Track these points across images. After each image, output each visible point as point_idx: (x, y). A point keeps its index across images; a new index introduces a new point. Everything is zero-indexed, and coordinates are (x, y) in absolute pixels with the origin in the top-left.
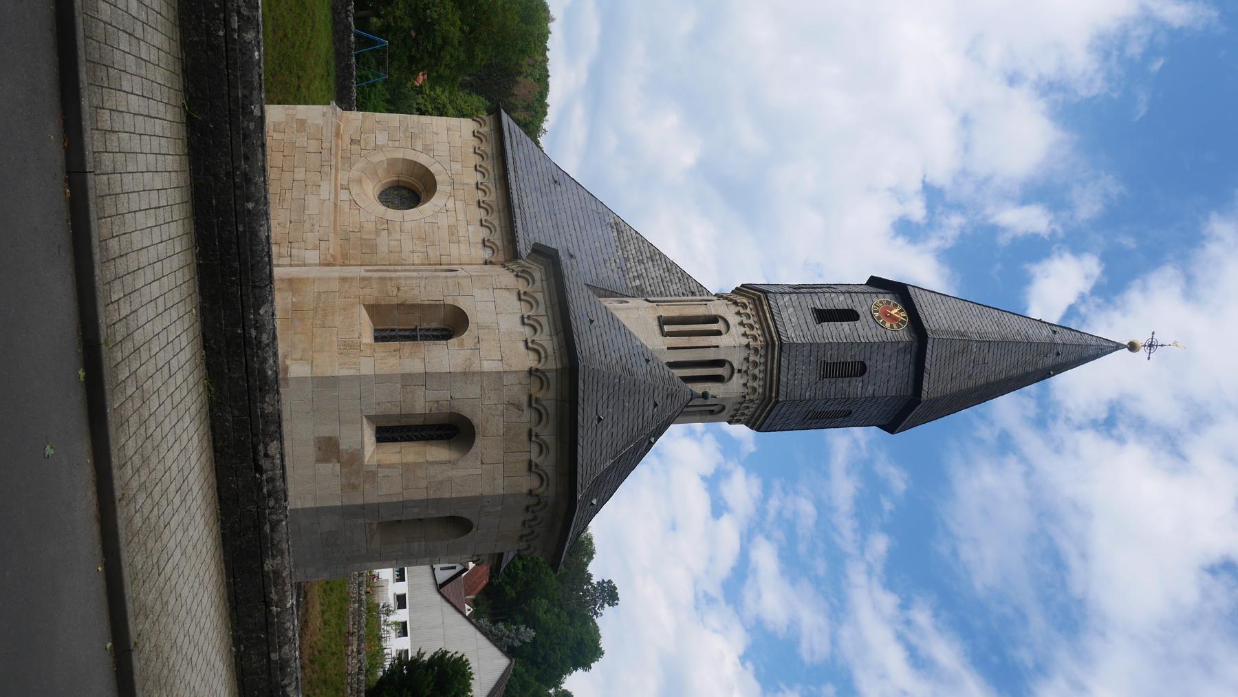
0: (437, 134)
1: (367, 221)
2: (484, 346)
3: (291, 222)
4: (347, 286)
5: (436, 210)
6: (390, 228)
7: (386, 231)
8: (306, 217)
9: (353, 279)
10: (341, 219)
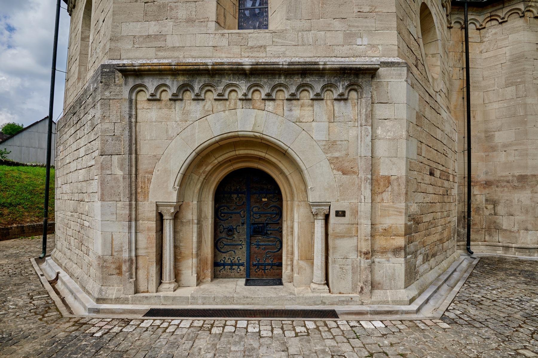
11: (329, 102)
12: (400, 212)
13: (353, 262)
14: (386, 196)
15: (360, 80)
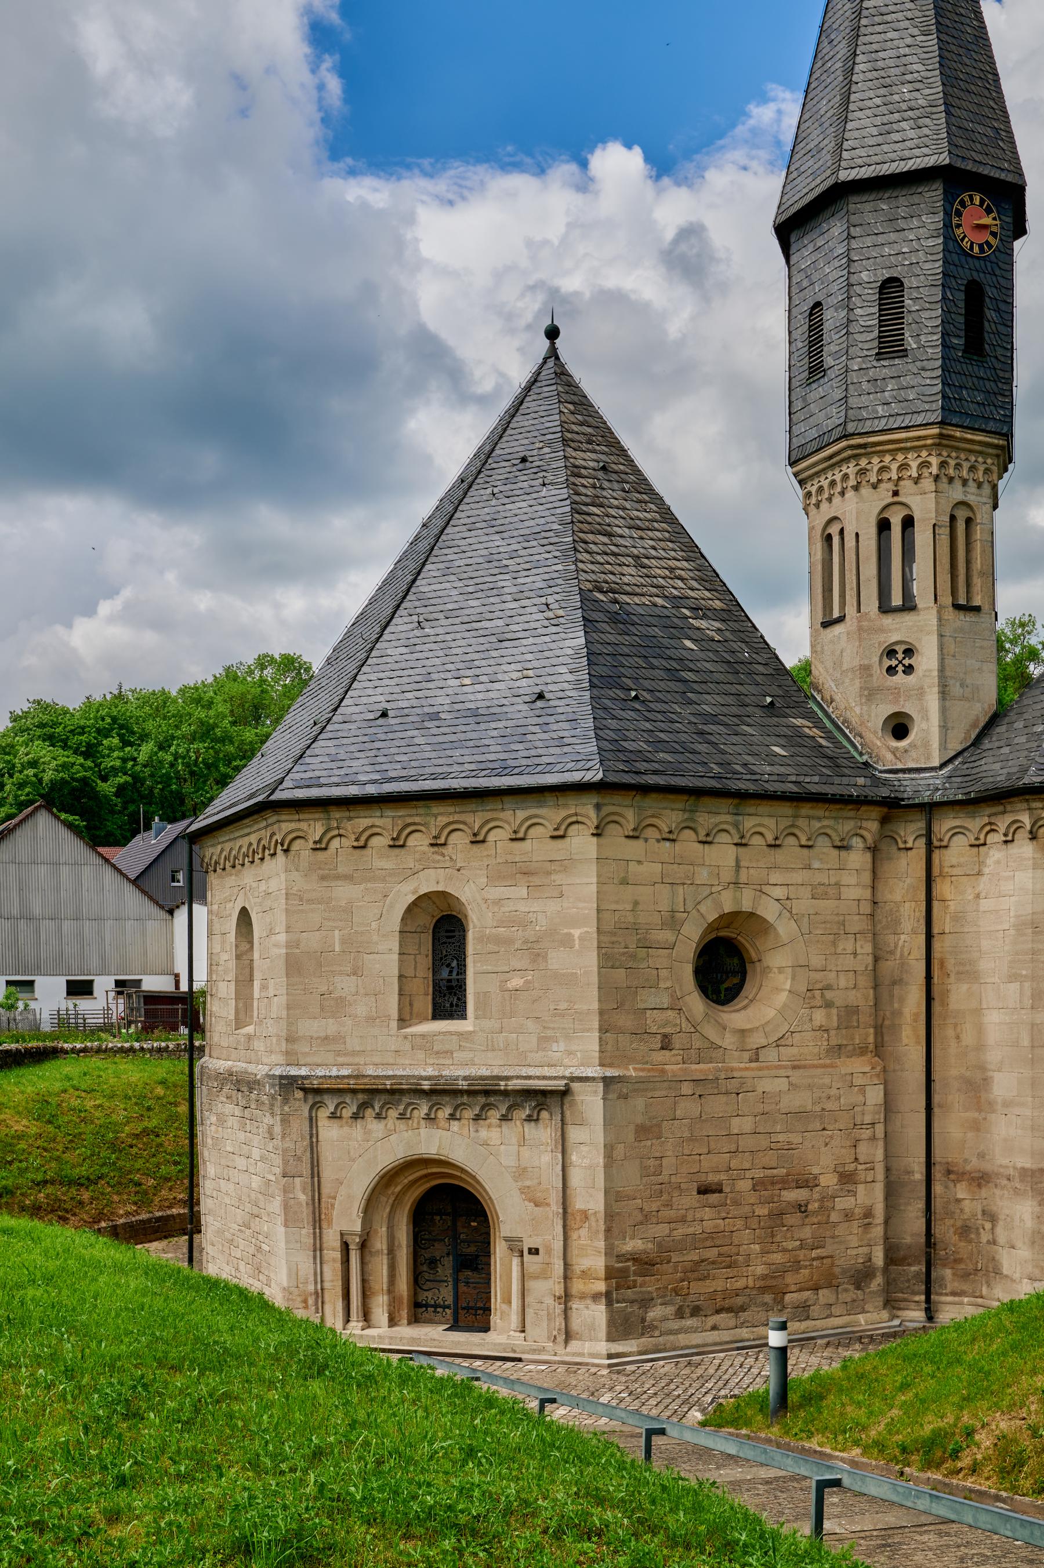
0: (636, 903)
3: (824, 1129)
5: (788, 914)
6: (819, 986)
7: (826, 992)
10: (808, 1058)
11: (518, 1123)
14: (583, 1232)
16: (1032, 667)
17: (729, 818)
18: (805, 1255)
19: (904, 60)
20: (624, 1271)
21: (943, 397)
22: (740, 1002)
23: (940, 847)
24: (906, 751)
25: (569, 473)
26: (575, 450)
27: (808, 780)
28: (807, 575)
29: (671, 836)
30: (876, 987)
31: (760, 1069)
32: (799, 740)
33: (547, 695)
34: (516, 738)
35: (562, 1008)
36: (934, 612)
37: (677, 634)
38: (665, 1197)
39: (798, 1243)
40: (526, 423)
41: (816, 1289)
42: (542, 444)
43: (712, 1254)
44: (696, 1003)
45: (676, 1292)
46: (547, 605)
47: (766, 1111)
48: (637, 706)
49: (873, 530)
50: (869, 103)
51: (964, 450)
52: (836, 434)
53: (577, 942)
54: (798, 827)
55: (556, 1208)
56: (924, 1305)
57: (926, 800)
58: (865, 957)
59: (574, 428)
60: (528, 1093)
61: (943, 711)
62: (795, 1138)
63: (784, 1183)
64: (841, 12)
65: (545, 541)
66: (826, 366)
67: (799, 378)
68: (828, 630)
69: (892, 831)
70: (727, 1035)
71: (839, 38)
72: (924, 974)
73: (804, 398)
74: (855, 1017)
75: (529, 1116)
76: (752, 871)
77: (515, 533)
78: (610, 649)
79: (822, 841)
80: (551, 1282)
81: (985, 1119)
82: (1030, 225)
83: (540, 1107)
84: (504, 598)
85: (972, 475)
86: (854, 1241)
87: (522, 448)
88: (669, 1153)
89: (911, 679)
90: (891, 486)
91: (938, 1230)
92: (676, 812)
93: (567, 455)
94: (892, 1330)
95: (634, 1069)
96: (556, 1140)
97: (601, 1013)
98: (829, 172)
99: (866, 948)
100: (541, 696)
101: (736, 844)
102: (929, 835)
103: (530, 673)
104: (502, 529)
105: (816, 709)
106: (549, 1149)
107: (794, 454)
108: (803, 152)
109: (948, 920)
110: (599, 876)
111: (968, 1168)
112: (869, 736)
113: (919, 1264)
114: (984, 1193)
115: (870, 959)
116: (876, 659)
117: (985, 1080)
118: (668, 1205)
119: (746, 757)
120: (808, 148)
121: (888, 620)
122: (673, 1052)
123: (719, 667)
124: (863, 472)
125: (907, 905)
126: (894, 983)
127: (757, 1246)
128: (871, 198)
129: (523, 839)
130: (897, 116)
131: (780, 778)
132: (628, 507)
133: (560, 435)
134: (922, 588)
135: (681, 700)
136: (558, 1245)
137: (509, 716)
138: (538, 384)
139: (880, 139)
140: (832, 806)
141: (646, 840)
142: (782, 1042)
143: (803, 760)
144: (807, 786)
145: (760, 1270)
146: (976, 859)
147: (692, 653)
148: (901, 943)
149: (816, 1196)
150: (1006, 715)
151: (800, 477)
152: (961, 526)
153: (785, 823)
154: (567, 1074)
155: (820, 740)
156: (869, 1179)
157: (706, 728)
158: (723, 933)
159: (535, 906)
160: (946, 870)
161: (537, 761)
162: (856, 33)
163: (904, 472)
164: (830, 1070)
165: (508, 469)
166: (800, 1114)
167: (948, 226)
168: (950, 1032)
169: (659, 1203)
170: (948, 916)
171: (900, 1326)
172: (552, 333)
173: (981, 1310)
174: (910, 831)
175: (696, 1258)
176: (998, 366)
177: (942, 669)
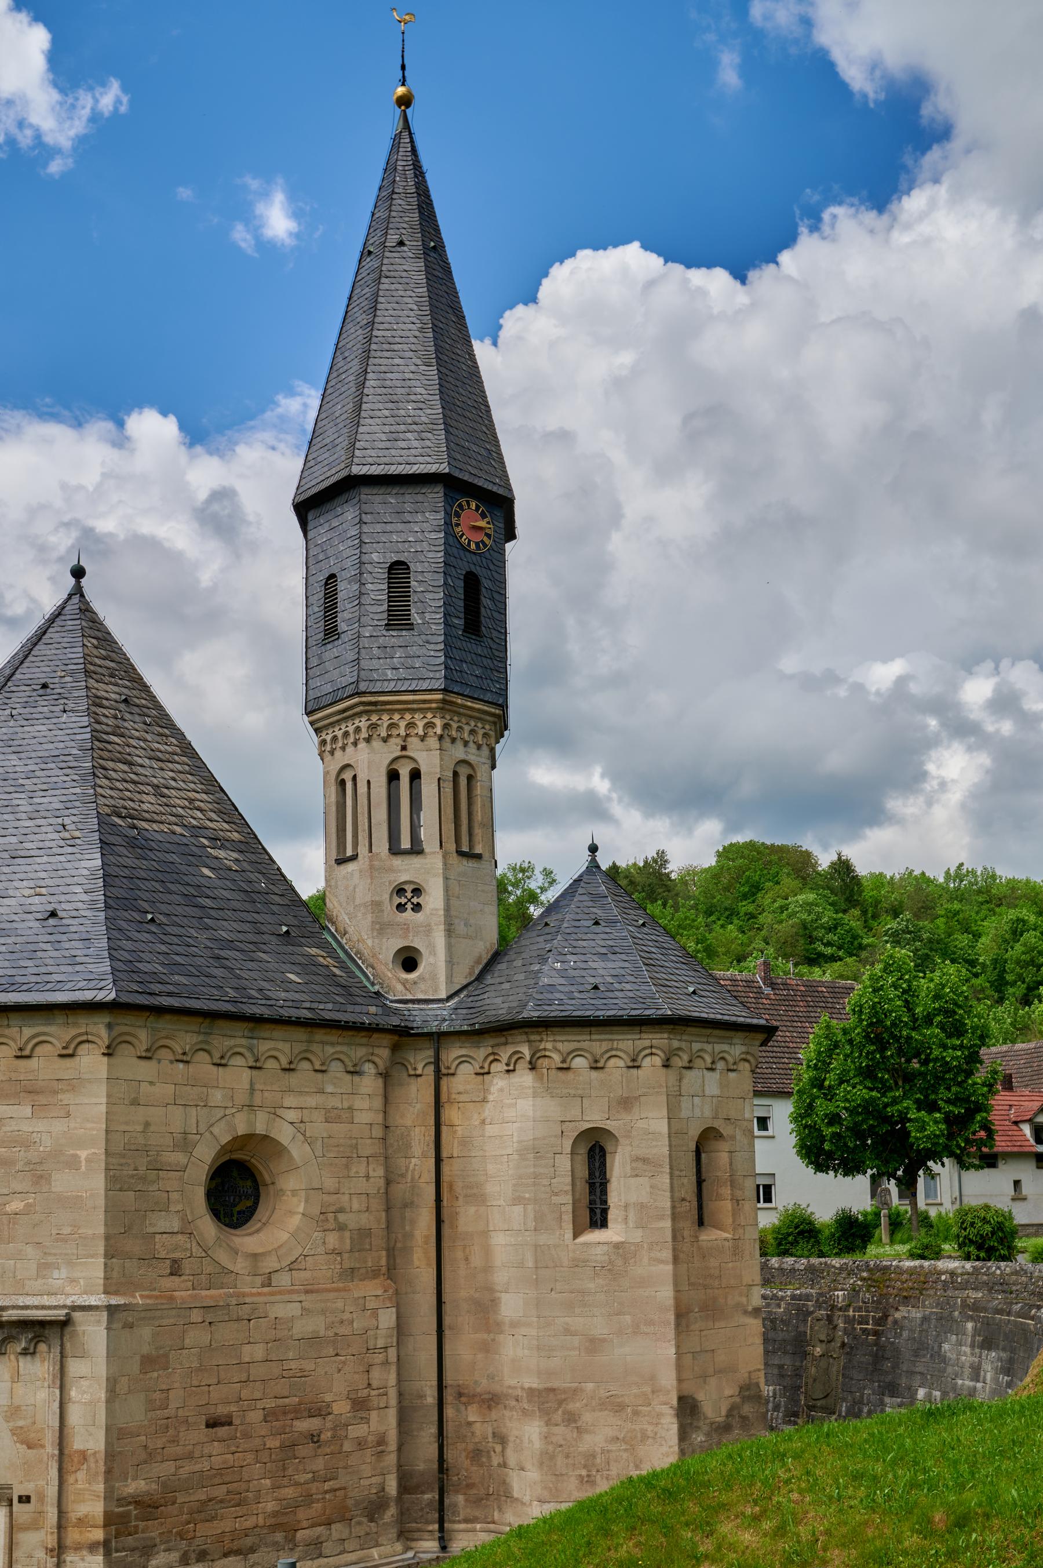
0: (147, 1124)
1: (324, 1243)
2: (733, 1114)
3: (337, 1355)
4: (681, 1256)
5: (301, 1137)
6: (332, 1209)
8: (331, 1333)
9: (674, 1250)
10: (322, 1282)
11: (12, 1357)
12: (98, 1496)
13: (39, 1561)
14: (81, 1475)
15: (47, 1332)
16: (532, 908)
17: (244, 1041)
18: (317, 1488)
19: (408, 383)
20: (124, 1517)
21: (446, 667)
22: (253, 1225)
23: (448, 1074)
24: (415, 983)
25: (90, 702)
26: (97, 681)
27: (321, 1006)
28: (322, 815)
29: (185, 1058)
30: (388, 1209)
31: (272, 1294)
32: (313, 968)
33: (60, 914)
34: (25, 954)
35: (65, 1232)
36: (440, 857)
37: (195, 862)
38: (171, 1432)
39: (310, 1475)
40: (48, 652)
41: (329, 1524)
42: (63, 674)
43: (220, 1492)
44: (208, 1227)
45: (181, 1536)
46: (64, 826)
47: (278, 1338)
48: (153, 928)
49: (384, 779)
50: (378, 413)
51: (465, 715)
52: (349, 691)
53: (83, 1163)
54: (312, 1052)
55: (52, 1449)
56: (437, 1535)
57: (434, 1030)
58: (378, 1179)
59: (97, 661)
60: (24, 1325)
61: (449, 947)
62: (308, 1365)
63: (298, 1412)
64: (354, 336)
65: (63, 765)
66: (339, 631)
67: (314, 638)
68: (342, 867)
69: (404, 1058)
70: (240, 1260)
71: (352, 357)
72: (434, 1197)
73: (320, 656)
74: (368, 1240)
75: (25, 1349)
76: (266, 1094)
77: (33, 755)
78: (127, 872)
79: (336, 1067)
80: (43, 1532)
81: (493, 1340)
82: (519, 531)
83: (38, 1339)
84: (18, 816)
85: (472, 737)
86: (367, 1470)
87: (43, 675)
88: (176, 1385)
89: (419, 916)
90: (399, 741)
91: (450, 1455)
92: (190, 1034)
93: (89, 685)
94: (406, 1563)
95: (142, 1296)
96: (54, 1375)
97: (107, 1238)
98: (343, 465)
99: (378, 1172)
100: (53, 914)
101: (250, 1067)
102: (437, 1062)
103: (43, 891)
104: (19, 749)
105: (330, 939)
106: (46, 1384)
107: (310, 704)
108: (320, 445)
109: (456, 1144)
110: (109, 1096)
111: (478, 1390)
112: (381, 968)
113: (432, 1491)
114: (494, 1415)
115: (382, 1182)
116: (387, 896)
117: (492, 1301)
118: (175, 1441)
119: (262, 983)
120: (325, 442)
121: (398, 862)
122: (183, 1278)
123: (235, 895)
124: (373, 727)
125: (417, 1129)
126: (405, 1206)
127: (268, 1481)
128: (381, 492)
129: (29, 1057)
130: (403, 428)
131: (294, 1004)
132: (149, 739)
133: (82, 666)
134: (428, 834)
135: (198, 925)
136: (52, 1491)
137: (19, 932)
138: (63, 618)
139: (388, 444)
140: (345, 1033)
141: (159, 1061)
142: (295, 1266)
143: (316, 987)
144: (321, 1013)
145: (271, 1506)
146: (481, 1087)
147: (210, 881)
148: (411, 1166)
149: (329, 1425)
150: (506, 954)
151: (316, 726)
152: (463, 782)
153: (298, 1047)
154: (68, 1303)
155: (334, 969)
156: (382, 1405)
157: (222, 953)
158: (236, 1156)
159: (41, 1126)
160: (453, 1096)
161: (47, 978)
162: (367, 356)
163: (411, 730)
164: (343, 1294)
165: (28, 694)
166: (314, 1340)
167: (448, 524)
168: (460, 1254)
169: (164, 1440)
170: (456, 1141)
171: (413, 1558)
172: (78, 573)
173: (492, 1537)
174: (420, 1059)
175: (203, 1497)
176: (494, 646)
177: (447, 909)
